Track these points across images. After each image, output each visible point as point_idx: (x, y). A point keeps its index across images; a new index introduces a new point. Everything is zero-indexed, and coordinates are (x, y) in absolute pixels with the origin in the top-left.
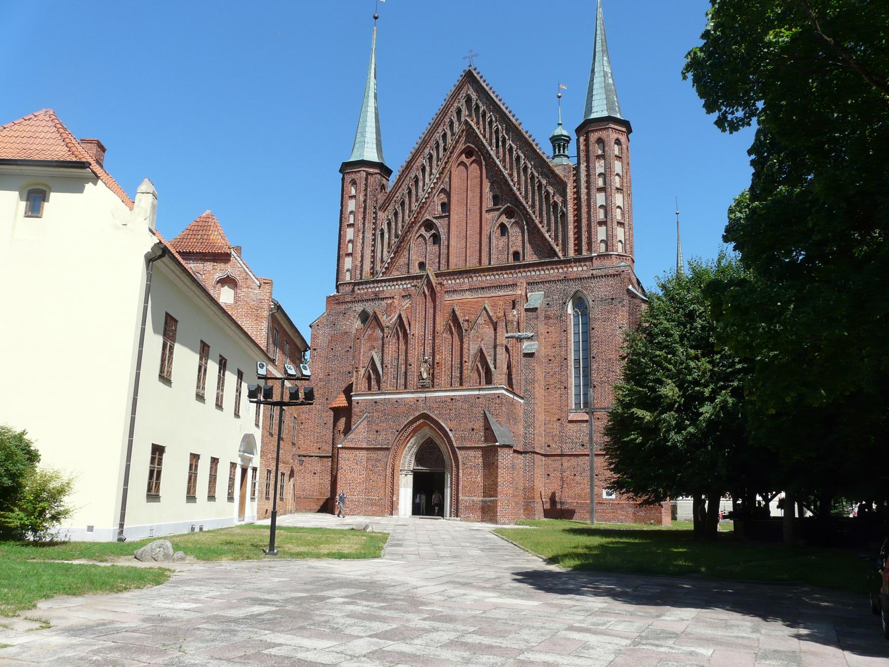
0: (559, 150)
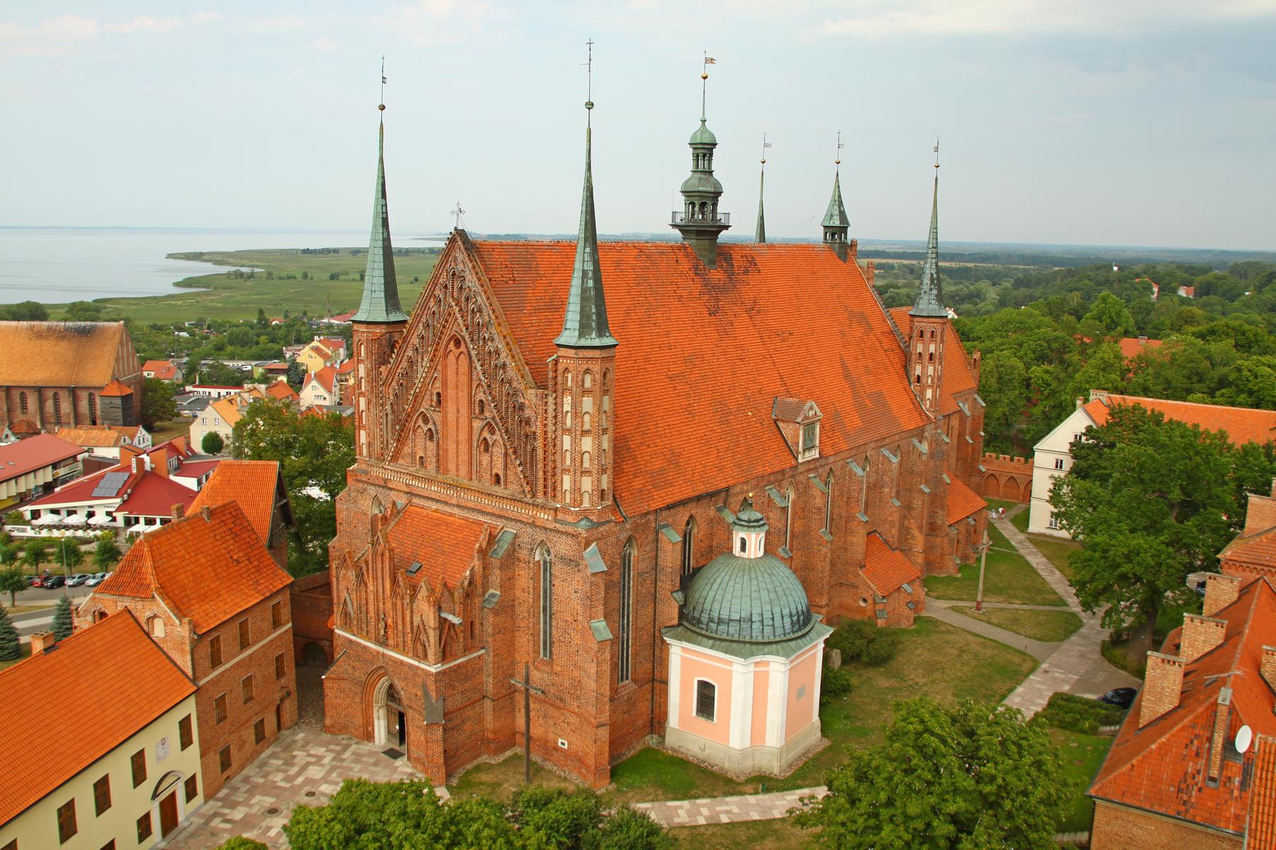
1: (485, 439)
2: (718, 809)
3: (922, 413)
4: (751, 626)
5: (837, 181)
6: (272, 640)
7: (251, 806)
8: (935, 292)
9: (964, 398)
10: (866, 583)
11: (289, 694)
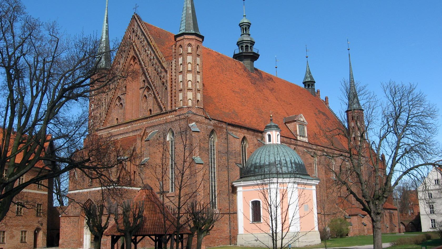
0: (246, 31)
5: (307, 64)
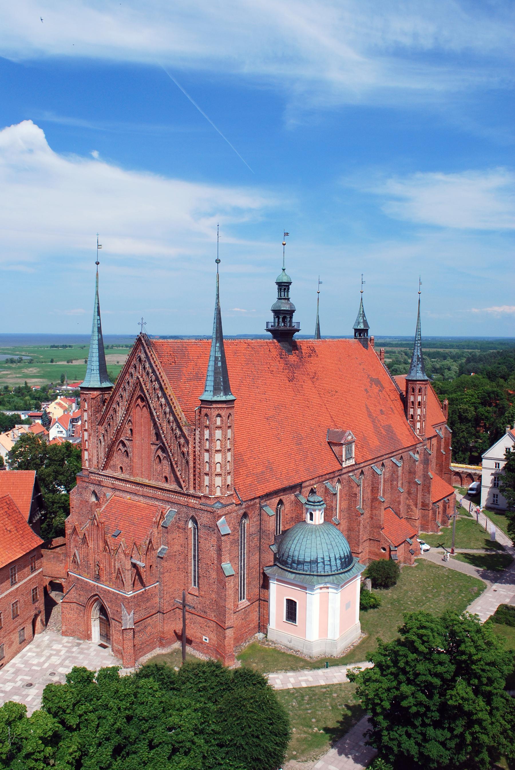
1: (158, 456)
2: (300, 678)
3: (414, 437)
4: (317, 565)
5: (362, 302)
6: (30, 579)
7: (16, 682)
8: (420, 366)
9: (439, 427)
10: (385, 539)
11: (40, 612)
